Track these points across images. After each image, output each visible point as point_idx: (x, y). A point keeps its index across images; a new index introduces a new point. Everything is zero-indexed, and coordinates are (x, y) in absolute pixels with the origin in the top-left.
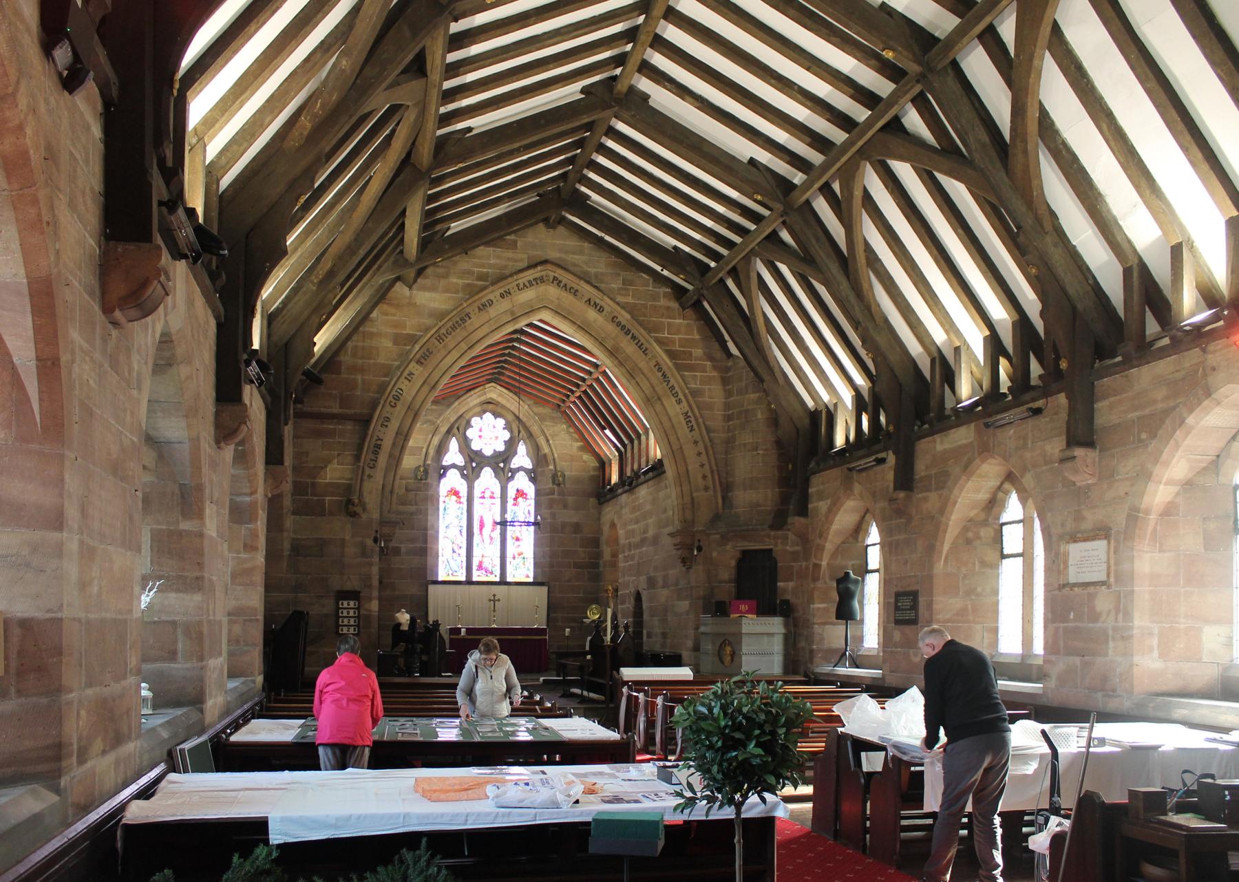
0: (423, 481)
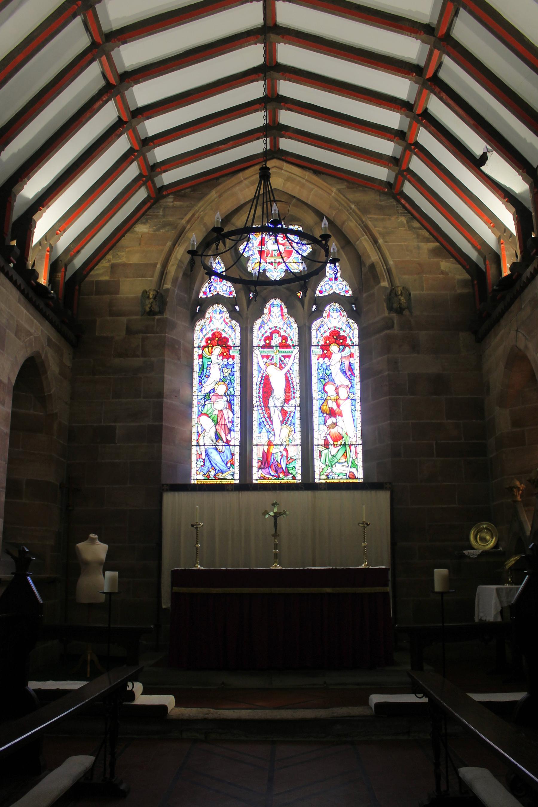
0: (157, 317)
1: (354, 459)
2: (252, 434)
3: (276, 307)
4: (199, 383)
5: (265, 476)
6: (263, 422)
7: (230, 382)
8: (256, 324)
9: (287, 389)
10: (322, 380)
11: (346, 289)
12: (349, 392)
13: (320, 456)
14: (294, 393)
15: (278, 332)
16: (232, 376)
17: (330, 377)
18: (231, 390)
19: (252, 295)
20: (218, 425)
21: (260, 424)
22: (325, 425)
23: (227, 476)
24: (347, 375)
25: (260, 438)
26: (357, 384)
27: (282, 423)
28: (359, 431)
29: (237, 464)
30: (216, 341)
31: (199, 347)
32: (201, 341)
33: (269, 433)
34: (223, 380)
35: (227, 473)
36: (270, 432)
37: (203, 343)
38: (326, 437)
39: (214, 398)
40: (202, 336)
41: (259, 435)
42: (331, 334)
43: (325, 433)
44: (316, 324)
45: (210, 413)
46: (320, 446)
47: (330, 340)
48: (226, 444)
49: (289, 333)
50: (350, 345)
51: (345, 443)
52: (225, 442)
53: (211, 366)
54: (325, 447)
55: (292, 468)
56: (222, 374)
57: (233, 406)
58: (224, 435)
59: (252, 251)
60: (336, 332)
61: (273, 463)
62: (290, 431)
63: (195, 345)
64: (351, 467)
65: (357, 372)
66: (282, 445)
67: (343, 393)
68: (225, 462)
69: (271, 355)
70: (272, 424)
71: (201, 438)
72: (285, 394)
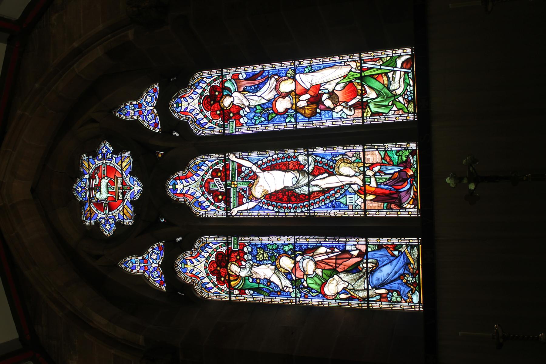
1: (381, 63)
2: (349, 219)
3: (177, 187)
4: (278, 295)
5: (412, 198)
6: (331, 202)
7: (276, 251)
8: (198, 213)
9: (284, 167)
10: (270, 118)
11: (152, 91)
12: (286, 78)
13: (379, 114)
14: (289, 157)
15: (208, 182)
16: (267, 247)
17: (265, 107)
18: (286, 249)
19: (162, 219)
20: (337, 269)
21: (334, 207)
22: (334, 109)
23: (413, 256)
24: (262, 82)
25: (354, 207)
26: (274, 66)
27: (331, 174)
28: (341, 58)
29: (395, 241)
30: (222, 270)
31: (230, 293)
32: (221, 290)
33: (347, 193)
34: (274, 260)
35: (408, 255)
36: (345, 190)
37: (225, 287)
38: (351, 106)
39: (299, 274)
40: (215, 289)
41: (350, 207)
42: (208, 109)
43: (345, 110)
44: (196, 130)
45: (321, 280)
46: (365, 115)
47: (216, 109)
48: (365, 257)
49: (207, 167)
50: (222, 80)
51: (358, 78)
52: (362, 259)
53: (255, 276)
54: (366, 108)
55: (398, 156)
56: (265, 262)
57: (310, 247)
58: (351, 259)
59: (110, 220)
60: (206, 102)
61: (391, 186)
62: (344, 162)
63: (227, 298)
64: (394, 66)
65: (258, 68)
66: (364, 173)
67: (287, 86)
68: (392, 258)
69: (238, 192)
70: (333, 188)
71: (355, 294)
72: (291, 170)
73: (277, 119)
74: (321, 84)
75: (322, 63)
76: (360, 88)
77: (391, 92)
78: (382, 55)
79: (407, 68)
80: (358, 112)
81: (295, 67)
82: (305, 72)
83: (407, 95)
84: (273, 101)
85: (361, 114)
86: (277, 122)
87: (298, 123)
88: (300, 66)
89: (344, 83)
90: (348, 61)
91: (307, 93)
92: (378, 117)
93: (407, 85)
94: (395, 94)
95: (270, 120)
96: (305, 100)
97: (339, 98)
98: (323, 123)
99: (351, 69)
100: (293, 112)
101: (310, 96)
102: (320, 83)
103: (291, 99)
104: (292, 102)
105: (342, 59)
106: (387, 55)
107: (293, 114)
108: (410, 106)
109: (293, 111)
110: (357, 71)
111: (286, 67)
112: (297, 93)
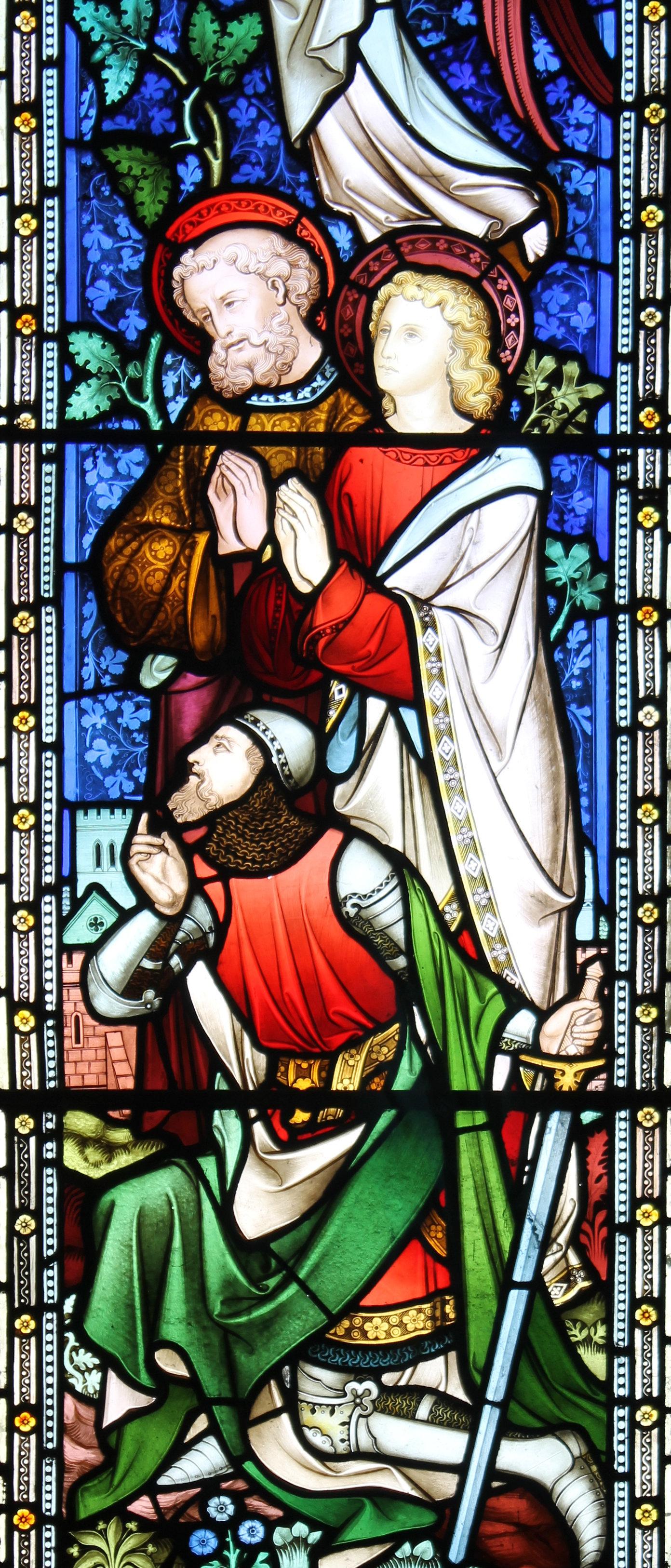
1: (559, 1296)
24: (496, 79)
28: (647, 913)
54: (140, 1137)
73: (111, 230)
74: (418, 704)
75: (623, 717)
76: (336, 1086)
77: (274, 1373)
78: (635, 1304)
79: (488, 1528)
80: (117, 1054)
81: (614, 440)
82: (555, 550)
83: (234, 1523)
84: (292, 200)
85: (91, 1080)
86: (83, 230)
87: (49, 458)
88: (623, 498)
89: (398, 932)
90: (610, 977)
91: (336, 552)
92: (51, 1242)
93: (332, 1520)
94: (258, 1411)
95: (100, 158)
96: (271, 538)
97: (261, 874)
98: (35, 709)
99: (530, 1005)
100: (161, 403)
101: (305, 588)
102: (431, 693)
103: (294, 388)
104: (268, 400)
105: (636, 921)
106: (629, 1351)
107: (148, 407)
108: (130, 1543)
109: (175, 409)
110: (502, 1066)
111: (624, 347)
112: (356, 453)
